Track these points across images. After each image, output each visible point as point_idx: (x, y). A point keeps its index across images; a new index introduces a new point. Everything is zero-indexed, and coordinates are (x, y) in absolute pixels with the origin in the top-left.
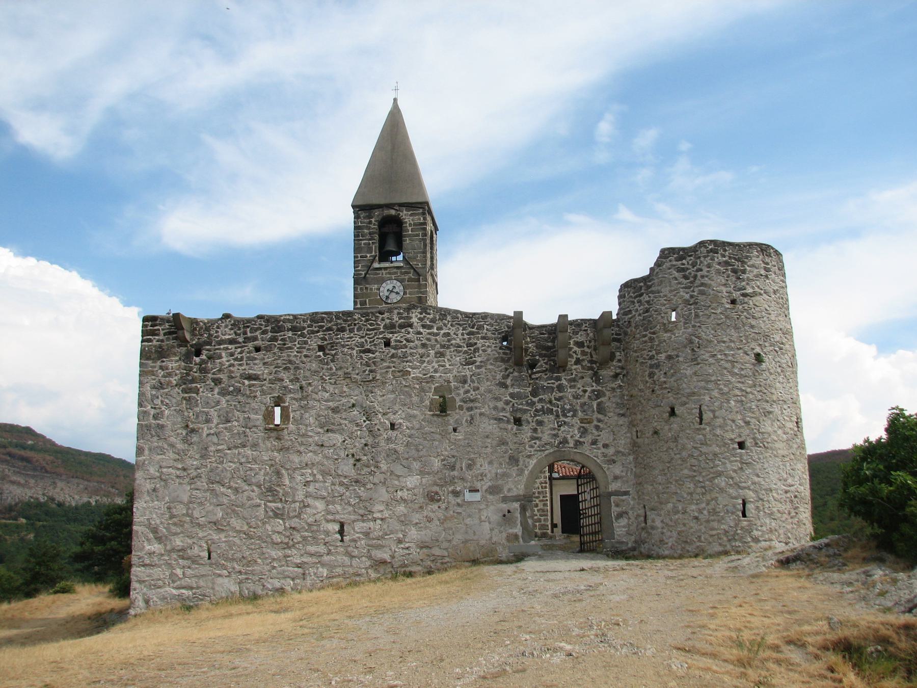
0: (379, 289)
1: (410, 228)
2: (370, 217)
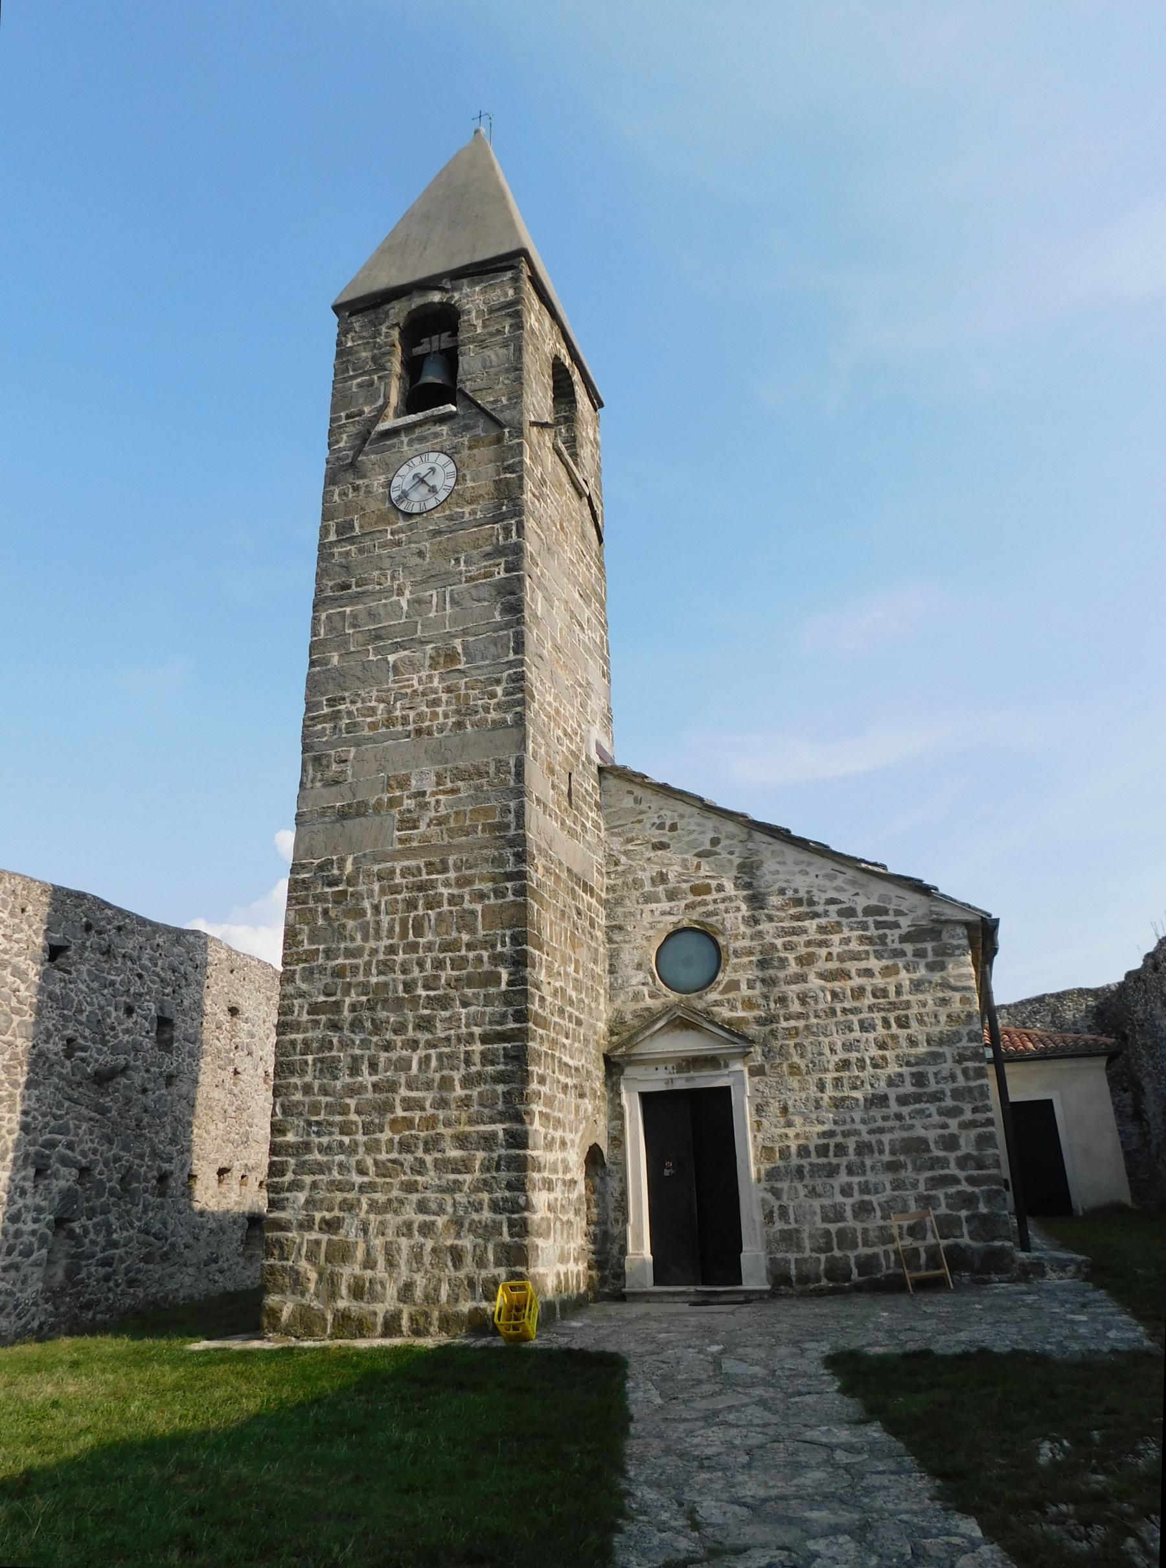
0: (389, 484)
2: (375, 324)
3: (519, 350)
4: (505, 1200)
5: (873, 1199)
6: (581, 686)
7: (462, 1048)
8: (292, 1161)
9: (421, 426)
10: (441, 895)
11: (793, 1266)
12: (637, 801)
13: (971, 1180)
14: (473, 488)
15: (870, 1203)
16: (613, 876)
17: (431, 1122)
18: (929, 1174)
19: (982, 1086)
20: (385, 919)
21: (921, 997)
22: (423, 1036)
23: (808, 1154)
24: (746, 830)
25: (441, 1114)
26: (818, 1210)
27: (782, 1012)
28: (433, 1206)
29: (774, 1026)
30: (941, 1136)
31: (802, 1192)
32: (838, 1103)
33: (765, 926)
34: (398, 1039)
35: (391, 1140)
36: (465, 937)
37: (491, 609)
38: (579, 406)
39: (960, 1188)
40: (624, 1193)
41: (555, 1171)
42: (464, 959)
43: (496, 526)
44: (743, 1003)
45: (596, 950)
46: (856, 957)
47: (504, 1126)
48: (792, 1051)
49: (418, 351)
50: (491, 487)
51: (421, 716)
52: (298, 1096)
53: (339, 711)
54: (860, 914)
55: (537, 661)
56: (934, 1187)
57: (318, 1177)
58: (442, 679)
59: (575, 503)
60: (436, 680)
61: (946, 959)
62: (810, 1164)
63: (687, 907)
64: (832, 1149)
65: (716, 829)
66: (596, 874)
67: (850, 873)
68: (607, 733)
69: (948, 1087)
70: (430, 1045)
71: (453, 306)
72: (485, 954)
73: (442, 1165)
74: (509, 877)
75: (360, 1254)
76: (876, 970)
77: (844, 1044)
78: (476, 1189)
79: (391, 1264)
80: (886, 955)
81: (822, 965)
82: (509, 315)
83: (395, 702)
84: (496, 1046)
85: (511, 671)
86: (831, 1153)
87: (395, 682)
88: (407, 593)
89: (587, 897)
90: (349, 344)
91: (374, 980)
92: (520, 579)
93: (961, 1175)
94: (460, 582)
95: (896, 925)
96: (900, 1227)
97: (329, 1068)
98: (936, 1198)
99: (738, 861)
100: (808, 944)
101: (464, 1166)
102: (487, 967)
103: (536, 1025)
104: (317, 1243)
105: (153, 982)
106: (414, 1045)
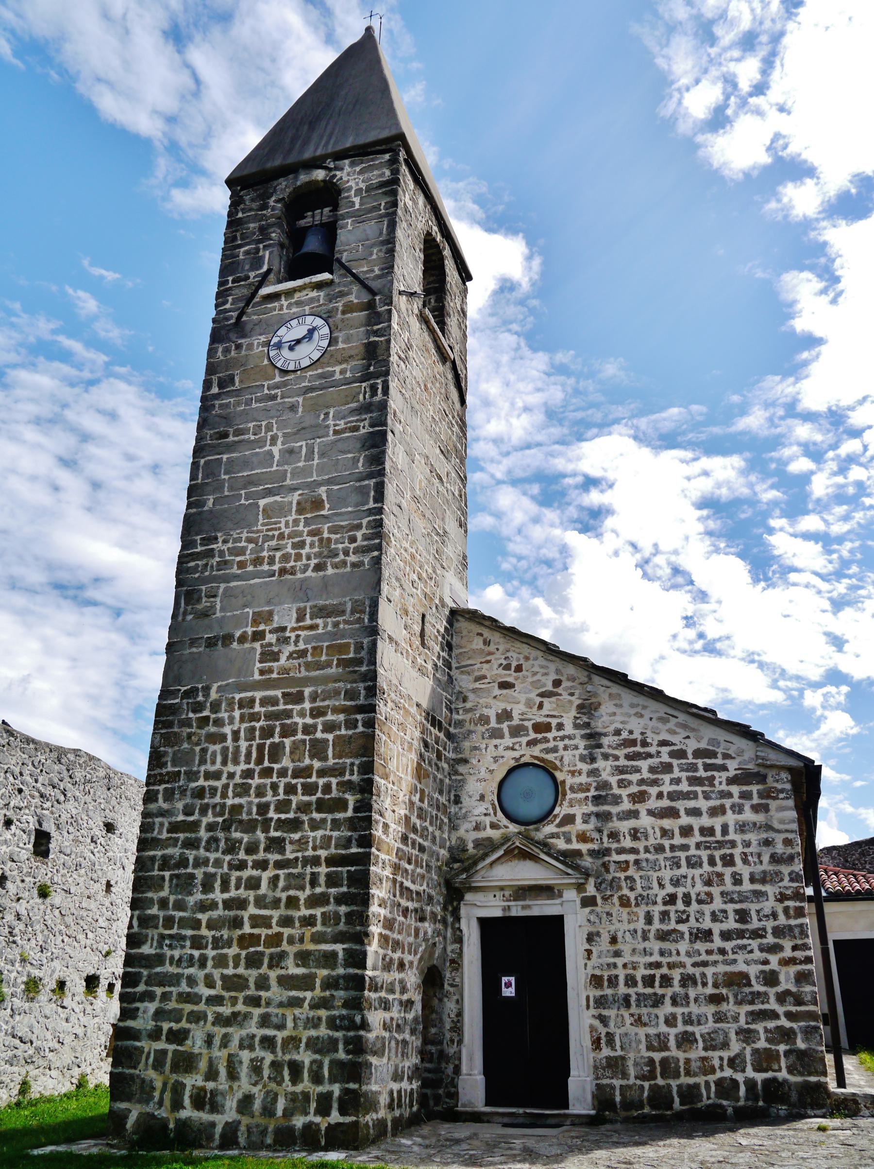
1: (357, 200)
3: (392, 226)
4: (342, 1018)
5: (697, 1030)
6: (438, 534)
7: (308, 870)
8: (145, 972)
9: (300, 291)
10: (296, 724)
11: (617, 1093)
12: (487, 643)
13: (790, 1016)
14: (343, 349)
15: (693, 1034)
16: (461, 712)
17: (275, 940)
18: (750, 1008)
19: (801, 925)
20: (243, 744)
21: (747, 837)
22: (273, 857)
23: (635, 984)
24: (586, 673)
25: (286, 932)
26: (643, 1039)
27: (614, 846)
28: (274, 1020)
29: (607, 858)
30: (762, 972)
31: (628, 1020)
32: (663, 936)
33: (600, 764)
34: (250, 859)
35: (237, 957)
36: (317, 764)
37: (355, 461)
38: (448, 279)
39: (779, 1023)
40: (460, 1014)
41: (392, 991)
42: (316, 785)
43: (364, 384)
44: (578, 836)
45: (441, 781)
46: (687, 796)
47: (345, 946)
48: (623, 884)
49: (302, 223)
50: (362, 349)
51: (286, 558)
52: (154, 911)
53: (213, 550)
54: (690, 756)
55: (396, 510)
56: (754, 1021)
57: (167, 989)
58: (307, 522)
59: (440, 367)
60: (302, 524)
61: (769, 801)
62: (637, 994)
63: (530, 743)
64: (658, 979)
65: (558, 671)
66: (444, 710)
67: (682, 717)
68: (461, 579)
69: (770, 925)
70: (279, 865)
71: (335, 184)
72: (334, 781)
73: (286, 982)
74: (361, 709)
75: (203, 1065)
76: (704, 809)
77: (671, 880)
78: (314, 1006)
79: (233, 1075)
80: (713, 796)
81: (653, 803)
82: (385, 193)
83: (264, 542)
84: (340, 869)
85: (371, 518)
86: (657, 984)
87: (263, 525)
88: (279, 442)
89: (435, 731)
90: (240, 215)
91: (229, 802)
92: (384, 434)
93: (781, 1010)
94: (328, 436)
95: (724, 768)
96: (721, 1059)
97: (184, 884)
98: (756, 1032)
99: (579, 702)
100: (642, 782)
101: (306, 983)
102: (334, 794)
103: (379, 850)
104: (164, 1052)
105: (33, 797)
106: (262, 865)
